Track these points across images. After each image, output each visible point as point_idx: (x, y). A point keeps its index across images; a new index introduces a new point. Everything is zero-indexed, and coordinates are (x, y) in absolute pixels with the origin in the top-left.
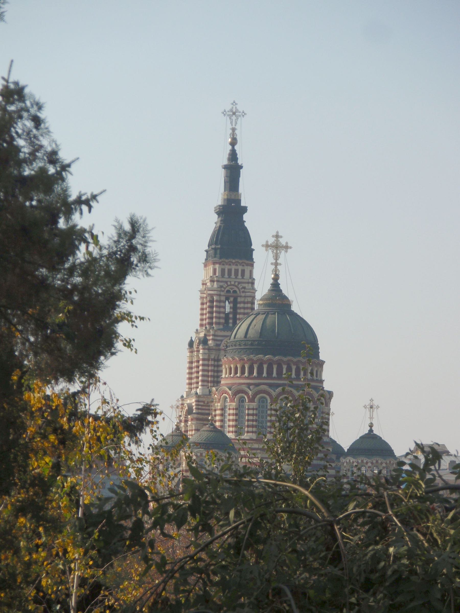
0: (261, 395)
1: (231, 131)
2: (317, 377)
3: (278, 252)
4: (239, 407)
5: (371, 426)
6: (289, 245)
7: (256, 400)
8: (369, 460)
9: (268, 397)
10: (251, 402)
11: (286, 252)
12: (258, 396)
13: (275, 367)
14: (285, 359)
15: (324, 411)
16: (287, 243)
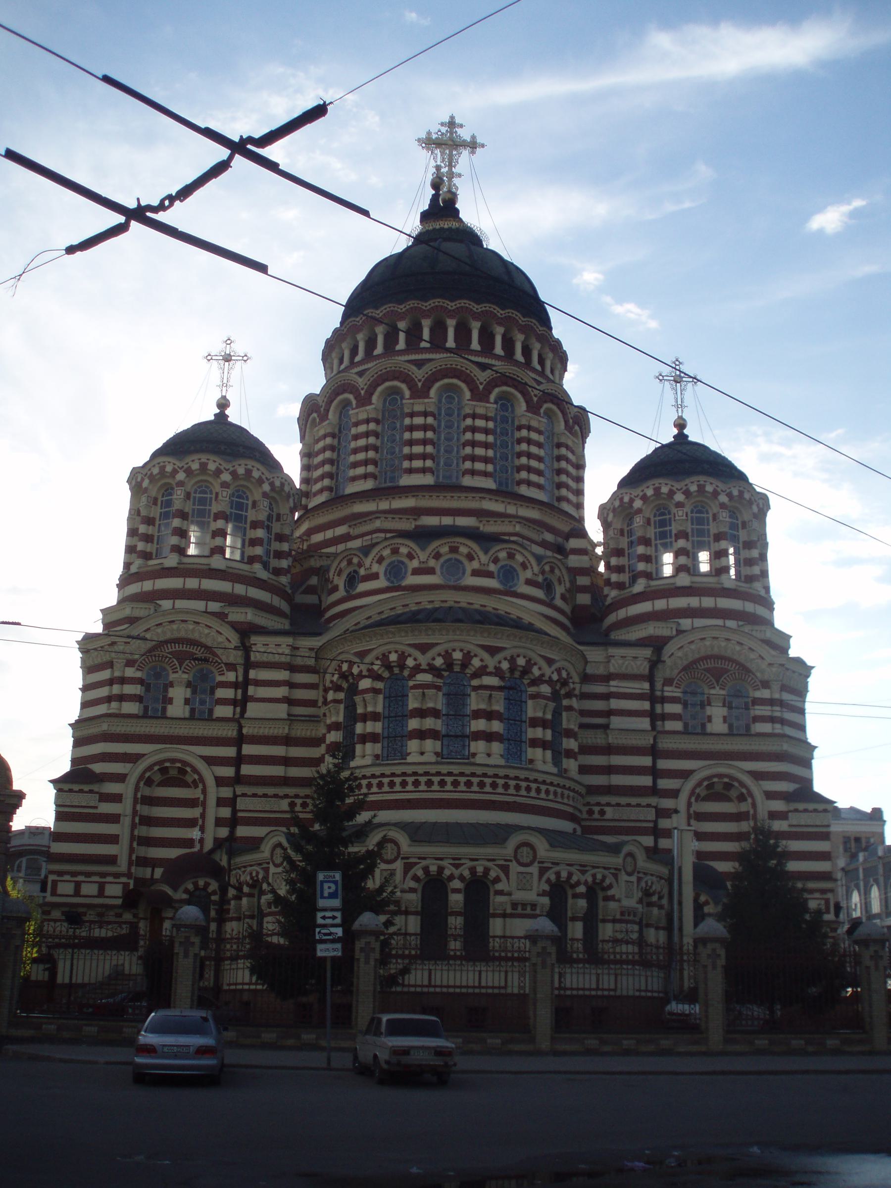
0: (387, 384)
1: (434, 170)
2: (541, 361)
3: (454, 153)
4: (340, 431)
5: (681, 425)
6: (479, 140)
7: (374, 399)
8: (677, 485)
9: (403, 386)
10: (363, 405)
11: (473, 153)
12: (380, 389)
13: (426, 324)
14: (451, 305)
15: (562, 441)
16: (473, 137)
